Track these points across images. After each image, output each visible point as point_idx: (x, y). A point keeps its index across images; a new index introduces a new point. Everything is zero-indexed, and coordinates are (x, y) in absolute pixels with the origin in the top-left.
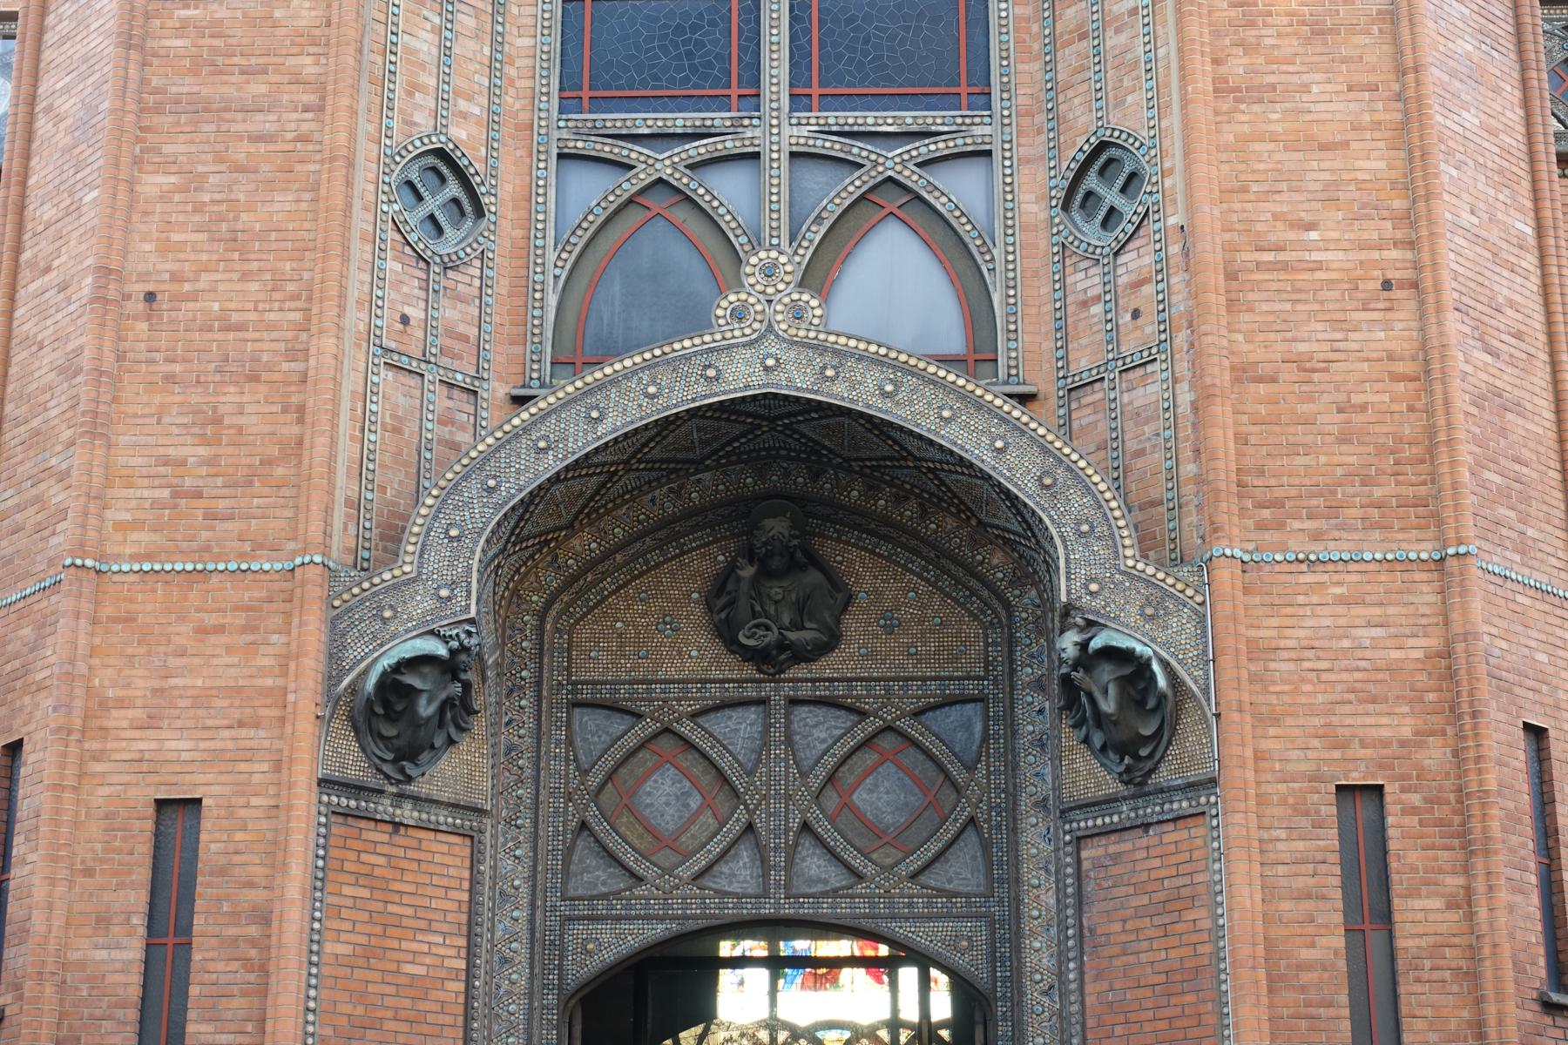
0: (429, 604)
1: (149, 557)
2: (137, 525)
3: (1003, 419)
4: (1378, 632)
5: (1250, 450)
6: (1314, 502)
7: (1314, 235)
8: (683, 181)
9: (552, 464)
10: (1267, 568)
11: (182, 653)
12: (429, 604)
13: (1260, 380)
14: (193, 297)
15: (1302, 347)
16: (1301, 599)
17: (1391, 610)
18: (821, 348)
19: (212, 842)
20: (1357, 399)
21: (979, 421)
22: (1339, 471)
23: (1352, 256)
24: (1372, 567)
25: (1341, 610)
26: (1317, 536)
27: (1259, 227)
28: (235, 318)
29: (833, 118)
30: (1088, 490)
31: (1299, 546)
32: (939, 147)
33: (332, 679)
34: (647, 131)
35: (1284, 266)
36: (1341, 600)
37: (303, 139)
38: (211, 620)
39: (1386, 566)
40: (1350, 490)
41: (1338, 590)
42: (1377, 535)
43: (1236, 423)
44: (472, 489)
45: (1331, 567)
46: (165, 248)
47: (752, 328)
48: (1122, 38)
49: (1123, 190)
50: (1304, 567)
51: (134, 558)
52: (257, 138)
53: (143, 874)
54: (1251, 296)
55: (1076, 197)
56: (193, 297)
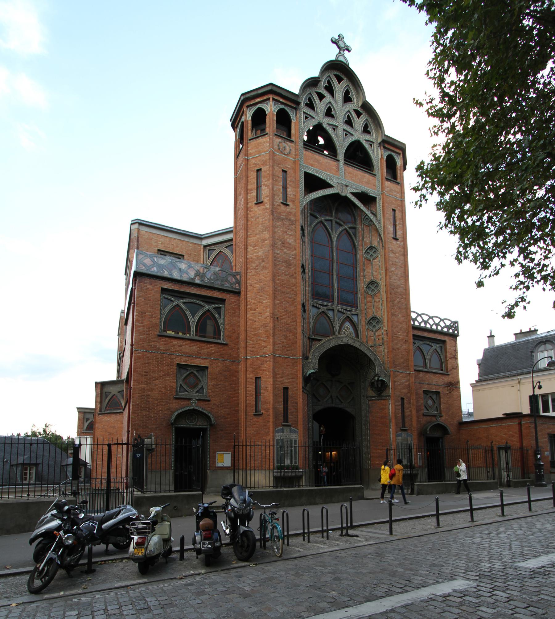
0: (313, 365)
1: (280, 355)
2: (278, 350)
8: (326, 312)
9: (325, 349)
11: (285, 368)
12: (313, 365)
14: (283, 319)
18: (353, 339)
19: (290, 393)
28: (288, 323)
29: (342, 306)
32: (353, 313)
33: (303, 373)
37: (294, 299)
38: (288, 364)
44: (317, 351)
46: (279, 311)
47: (346, 335)
48: (377, 304)
49: (376, 323)
51: (278, 354)
52: (289, 298)
53: (282, 397)
55: (369, 323)
56: (283, 319)
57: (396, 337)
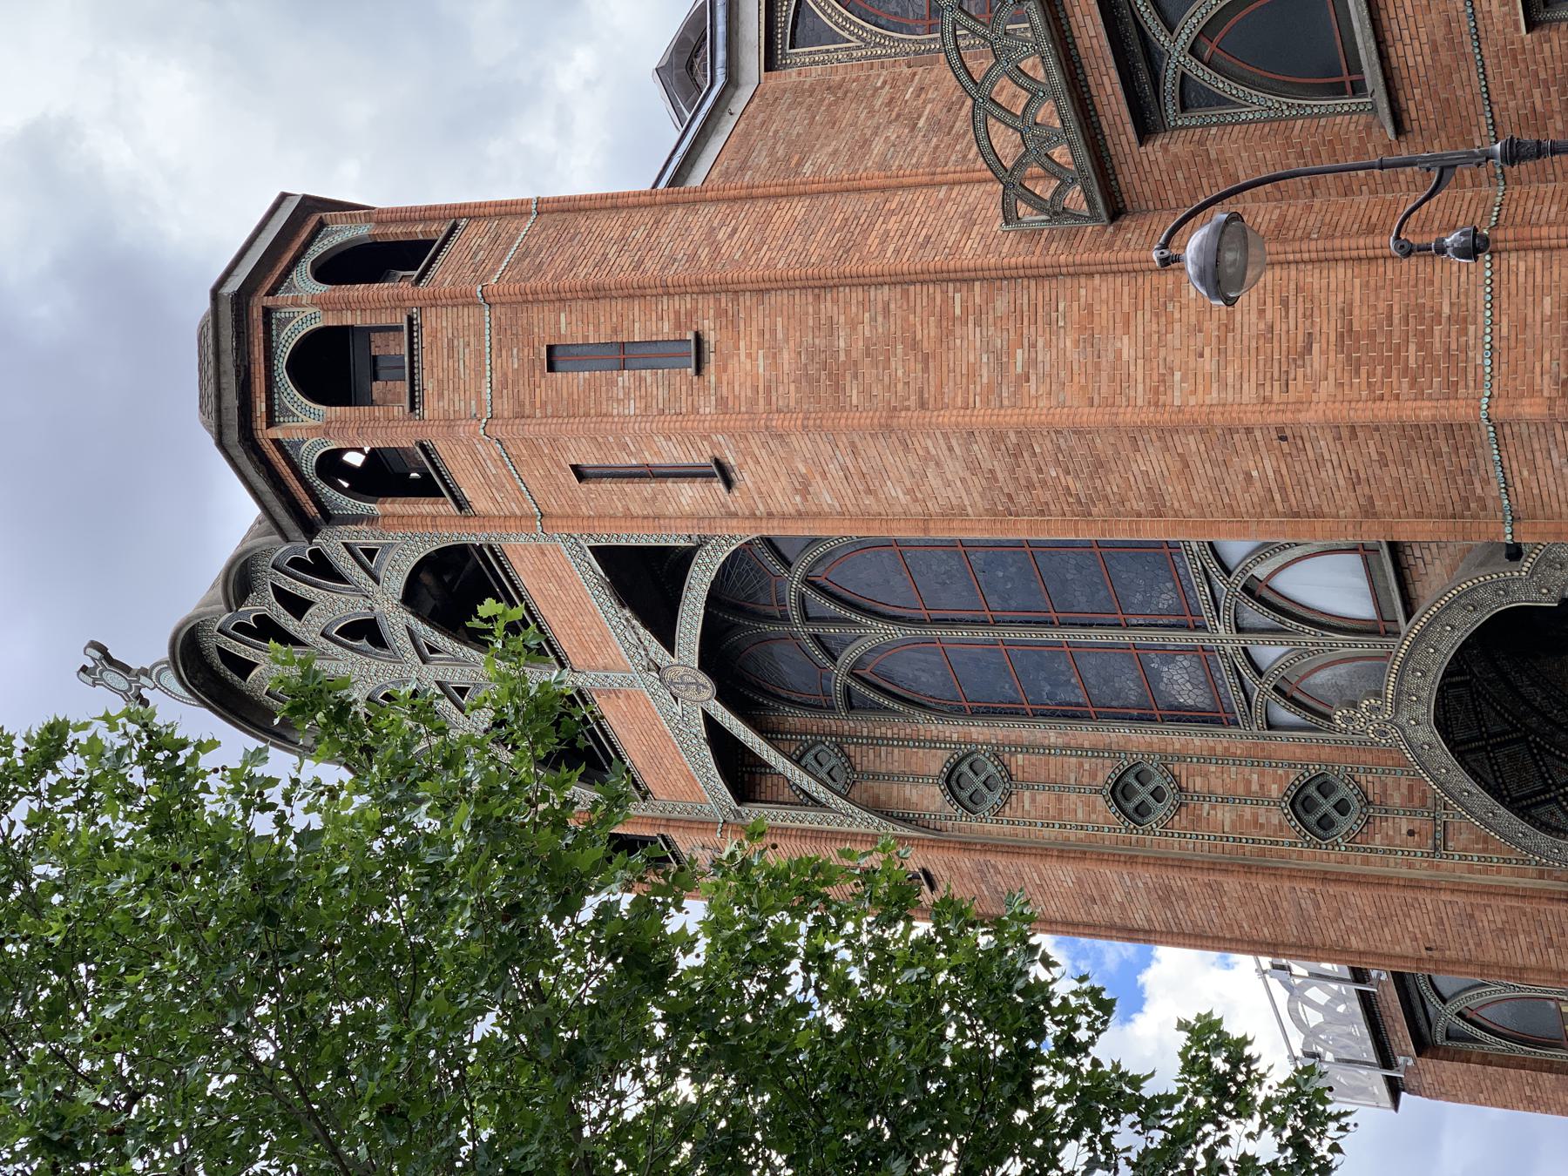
3: (1430, 625)
4: (1554, 454)
5: (1426, 511)
6: (1460, 482)
7: (1255, 473)
10: (1515, 507)
13: (1372, 504)
15: (1342, 482)
16: (1536, 491)
17: (1536, 446)
20: (1375, 457)
21: (1433, 638)
22: (1433, 468)
23: (1265, 455)
24: (1504, 454)
25: (1540, 472)
26: (1486, 482)
27: (1255, 499)
30: (1474, 589)
31: (1495, 488)
34: (1242, 694)
35: (1283, 489)
36: (1534, 469)
39: (1502, 448)
40: (1446, 463)
41: (1525, 473)
42: (1479, 451)
43: (1408, 516)
45: (1509, 476)
50: (1511, 489)
54: (1309, 505)
57: (1282, 489)
